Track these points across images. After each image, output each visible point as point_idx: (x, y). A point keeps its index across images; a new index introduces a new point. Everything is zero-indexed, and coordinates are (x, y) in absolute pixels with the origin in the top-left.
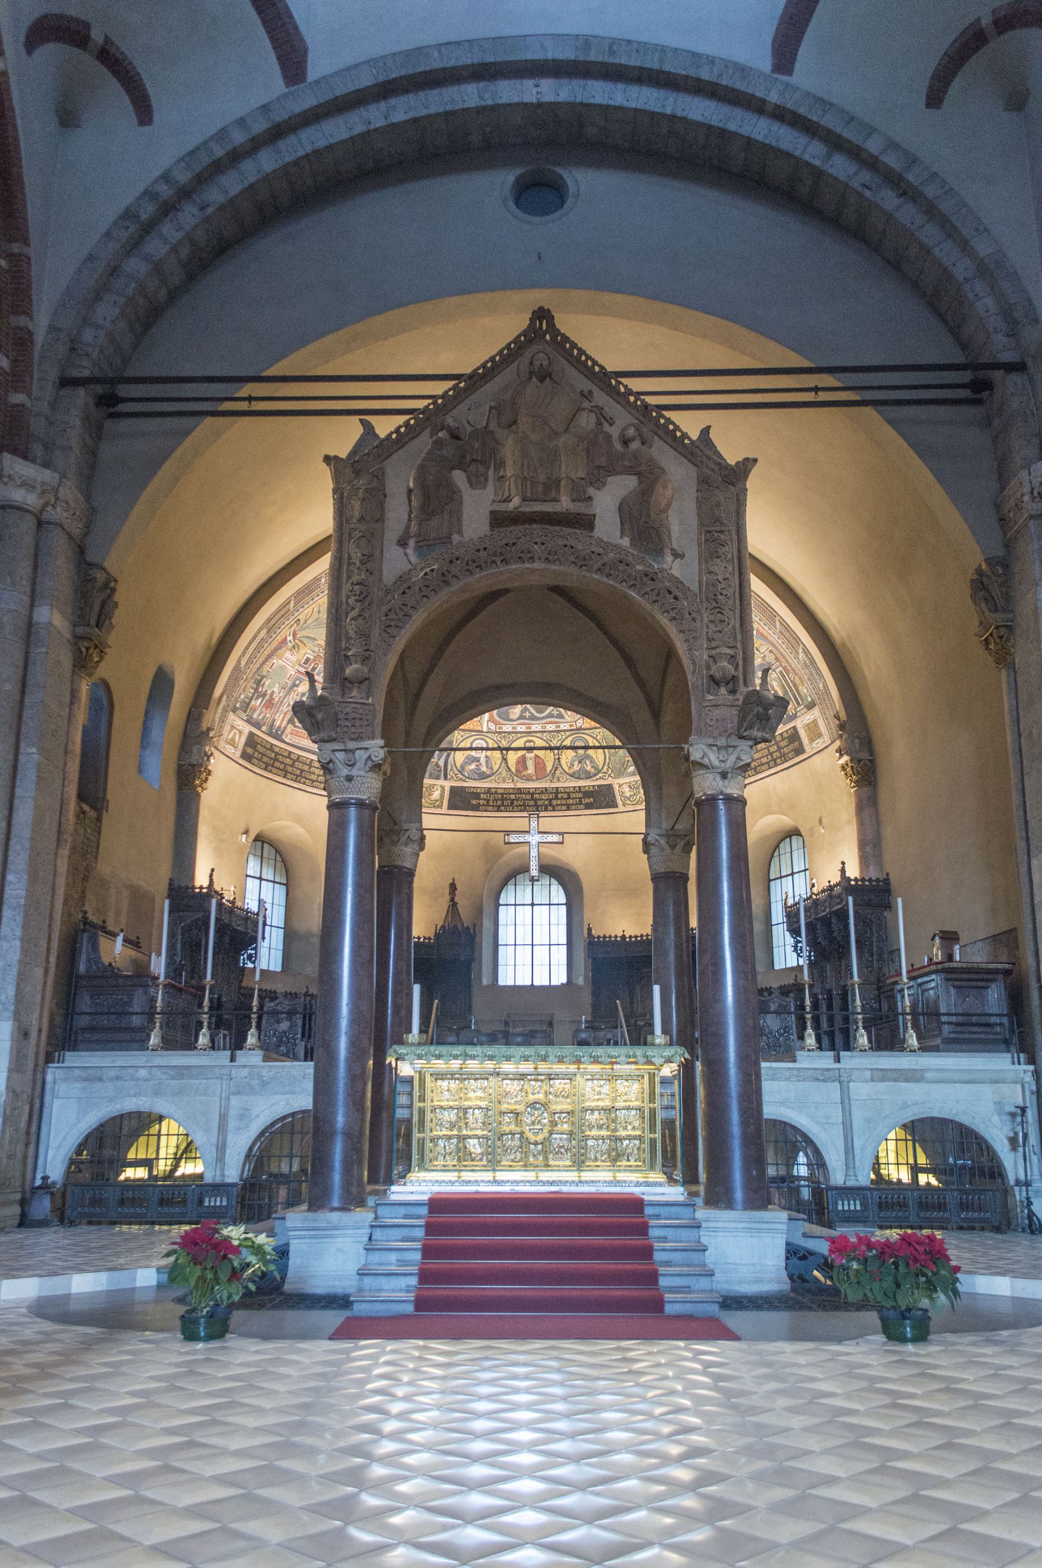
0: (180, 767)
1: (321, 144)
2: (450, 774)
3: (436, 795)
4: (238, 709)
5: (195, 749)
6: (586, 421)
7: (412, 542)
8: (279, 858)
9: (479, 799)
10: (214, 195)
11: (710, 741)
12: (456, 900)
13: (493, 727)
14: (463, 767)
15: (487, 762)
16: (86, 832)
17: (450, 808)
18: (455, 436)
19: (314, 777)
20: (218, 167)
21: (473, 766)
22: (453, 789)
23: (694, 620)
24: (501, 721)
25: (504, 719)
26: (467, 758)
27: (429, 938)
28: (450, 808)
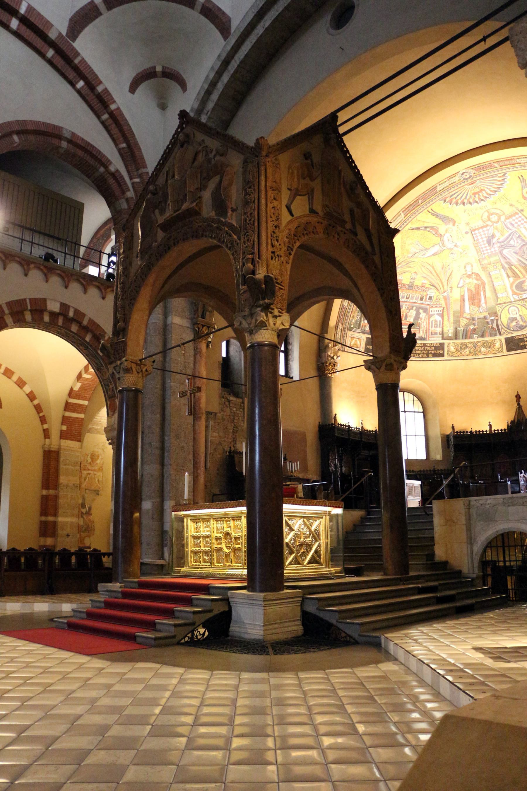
0: (318, 365)
1: (242, 57)
2: (502, 331)
3: (498, 345)
4: (353, 328)
5: (323, 355)
6: (201, 158)
8: (415, 398)
9: (524, 341)
10: (210, 105)
11: (243, 314)
12: (521, 404)
13: (516, 297)
14: (508, 325)
15: (521, 318)
16: (231, 409)
17: (508, 351)
18: (154, 194)
19: (419, 352)
21: (514, 323)
22: (507, 340)
23: (237, 244)
24: (520, 292)
25: (521, 291)
26: (509, 319)
27: (505, 430)
28: (508, 351)
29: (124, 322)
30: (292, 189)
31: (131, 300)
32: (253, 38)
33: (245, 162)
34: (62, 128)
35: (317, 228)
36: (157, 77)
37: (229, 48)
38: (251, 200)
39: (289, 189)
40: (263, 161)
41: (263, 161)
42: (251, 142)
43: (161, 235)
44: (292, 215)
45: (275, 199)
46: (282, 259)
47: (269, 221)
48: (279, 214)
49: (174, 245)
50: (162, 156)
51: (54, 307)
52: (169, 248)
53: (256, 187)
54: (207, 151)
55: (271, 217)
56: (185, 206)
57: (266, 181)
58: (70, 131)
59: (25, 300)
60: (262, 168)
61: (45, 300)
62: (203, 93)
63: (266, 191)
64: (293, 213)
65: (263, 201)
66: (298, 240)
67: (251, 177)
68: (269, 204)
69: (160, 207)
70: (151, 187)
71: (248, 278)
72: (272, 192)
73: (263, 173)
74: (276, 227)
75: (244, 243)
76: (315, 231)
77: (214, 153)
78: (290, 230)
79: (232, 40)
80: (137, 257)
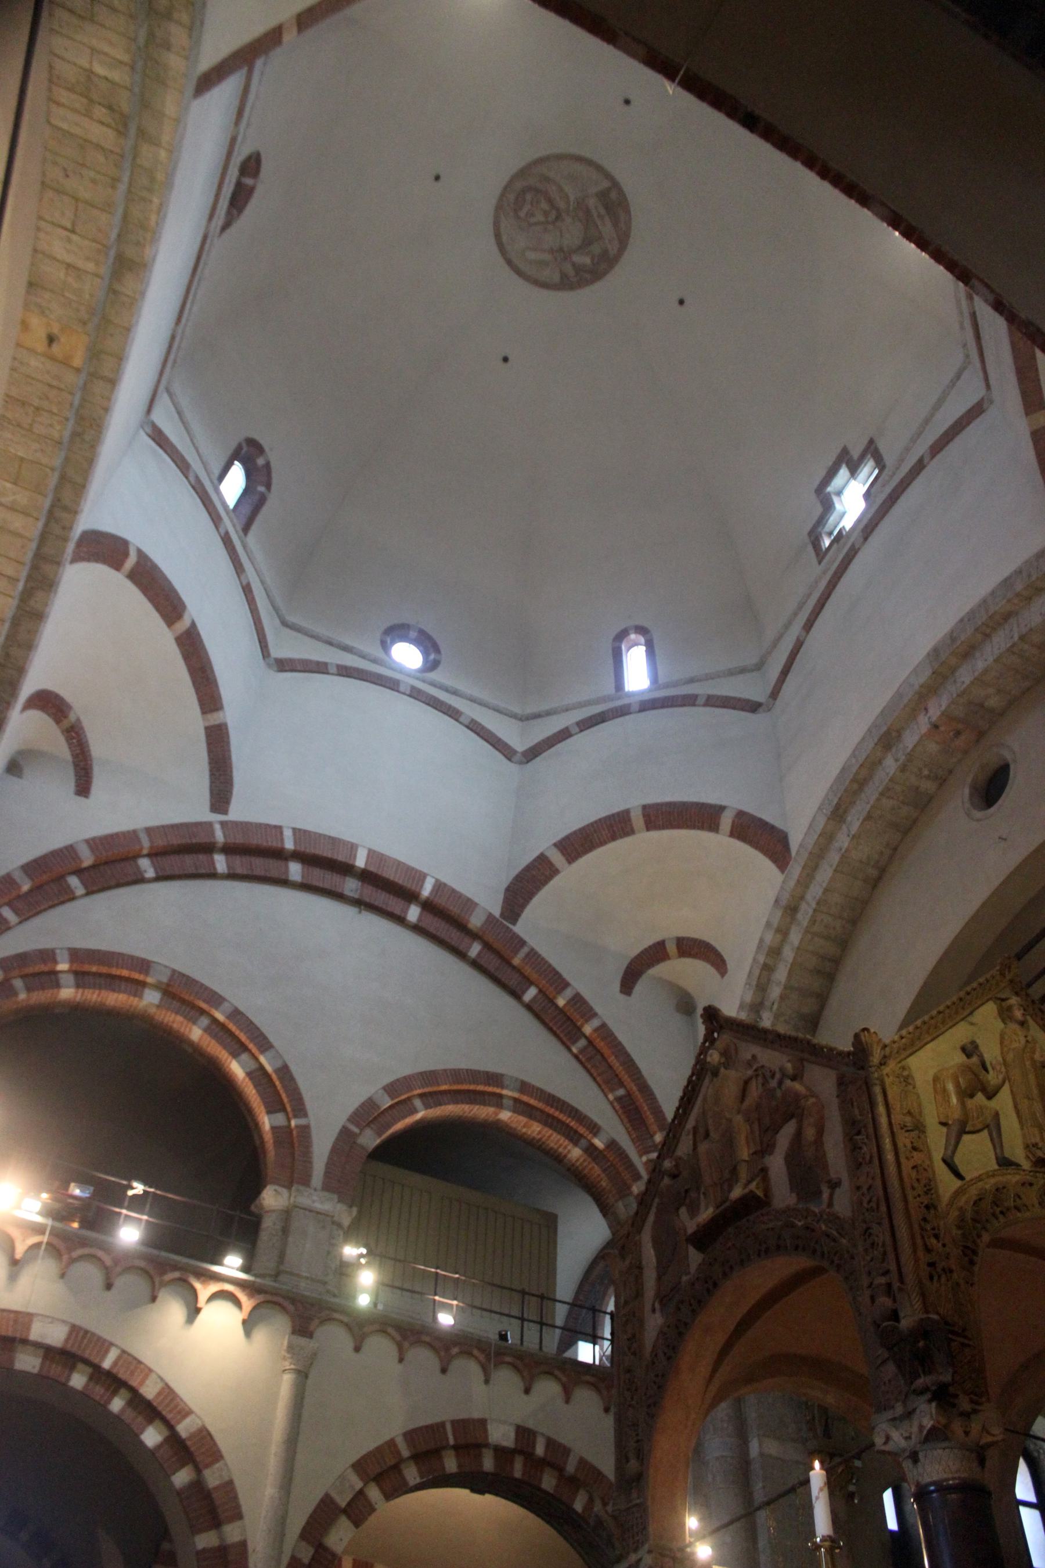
6: (755, 1091)
7: (657, 1306)
11: (889, 1414)
18: (674, 1177)
20: (768, 969)
29: (638, 1458)
30: (950, 1122)
31: (649, 1406)
32: (834, 857)
33: (841, 1082)
34: (502, 1075)
35: (1023, 1196)
36: (669, 959)
37: (792, 883)
38: (864, 1158)
39: (943, 1124)
40: (876, 1075)
41: (876, 1075)
42: (845, 1045)
43: (695, 1257)
44: (959, 1176)
45: (915, 1149)
46: (955, 1276)
47: (910, 1198)
48: (930, 1180)
49: (725, 1274)
50: (682, 1098)
51: (501, 1434)
52: (715, 1285)
53: (871, 1130)
54: (764, 1077)
55: (913, 1188)
56: (737, 1193)
57: (889, 1116)
58: (517, 1079)
59: (442, 1425)
60: (877, 1090)
61: (483, 1422)
62: (757, 972)
63: (893, 1134)
64: (963, 1173)
65: (890, 1157)
66: (984, 1228)
67: (857, 1112)
68: (903, 1160)
69: (687, 1201)
70: (667, 1164)
71: (886, 1327)
72: (907, 1134)
73: (880, 1099)
74: (927, 1207)
75: (866, 1250)
76: (1019, 1202)
77: (778, 1076)
78: (961, 1209)
79: (796, 869)
80: (654, 1311)
